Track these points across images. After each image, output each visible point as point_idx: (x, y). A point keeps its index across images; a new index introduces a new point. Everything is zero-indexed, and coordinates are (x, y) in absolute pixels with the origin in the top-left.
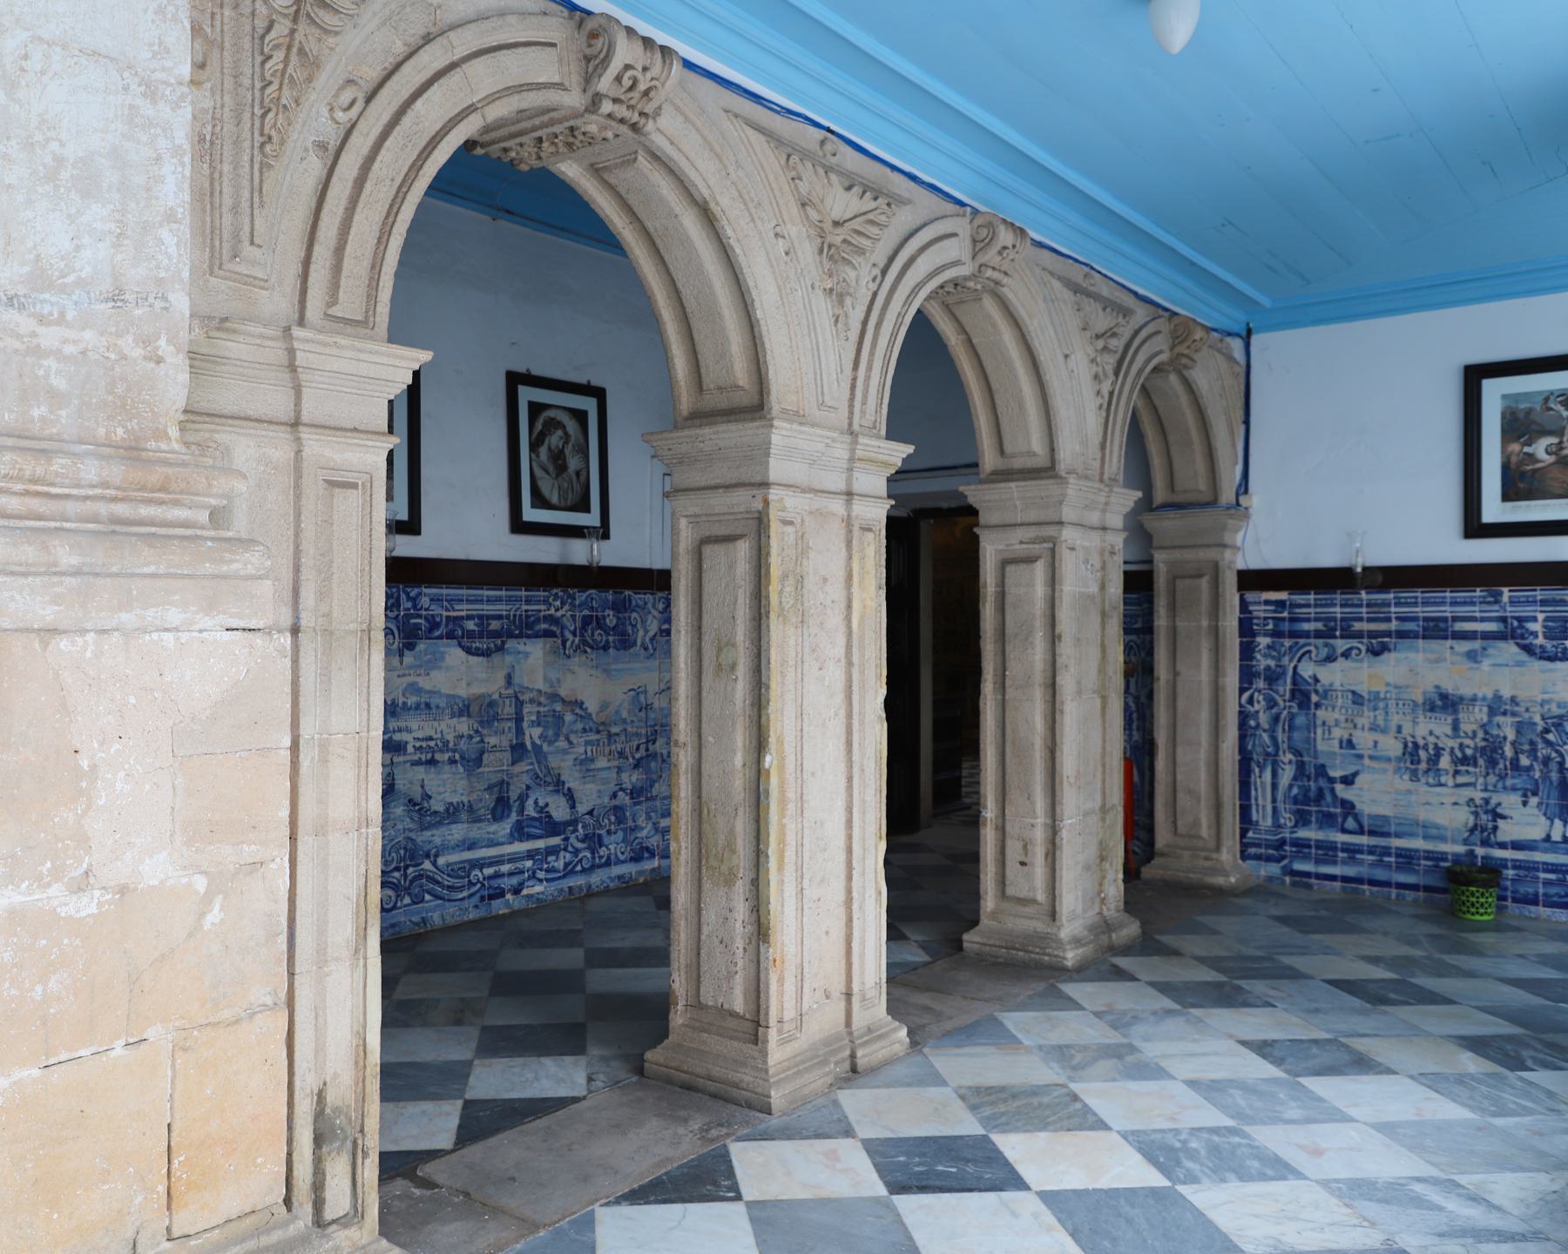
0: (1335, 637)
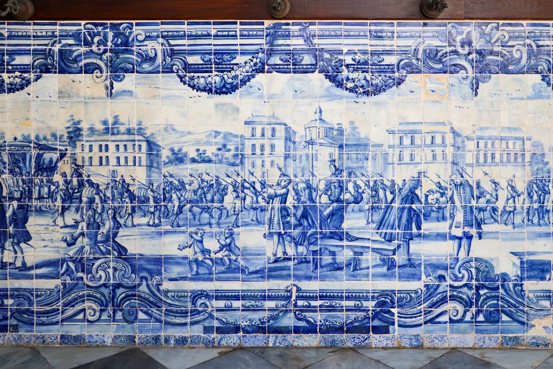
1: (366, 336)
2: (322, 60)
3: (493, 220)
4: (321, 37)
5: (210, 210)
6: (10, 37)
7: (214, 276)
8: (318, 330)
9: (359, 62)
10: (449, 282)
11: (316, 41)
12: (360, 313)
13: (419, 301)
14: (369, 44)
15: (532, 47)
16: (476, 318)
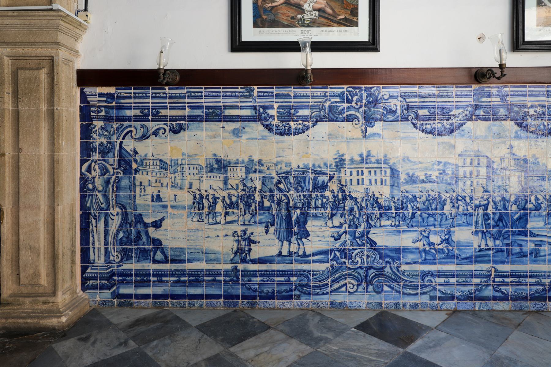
0: (149, 121)
1: (544, 303)
4: (512, 96)
5: (434, 216)
6: (295, 97)
7: (437, 261)
8: (510, 299)
11: (508, 99)
12: (540, 287)
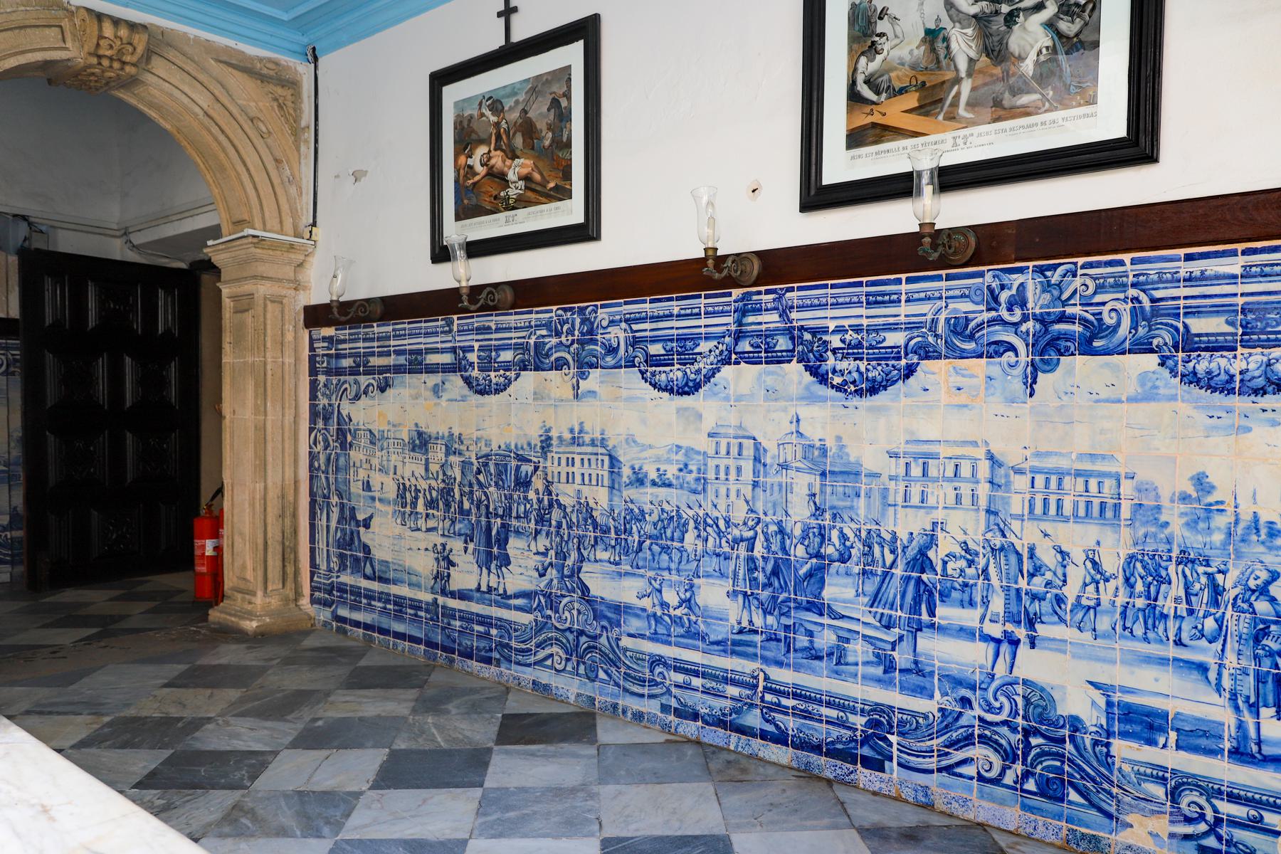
1: (851, 767)
2: (802, 344)
3: (1056, 619)
4: (801, 308)
9: (850, 344)
10: (978, 711)
11: (794, 315)
12: (845, 731)
13: (930, 732)
14: (863, 315)
15: (1140, 302)
16: (1022, 784)
